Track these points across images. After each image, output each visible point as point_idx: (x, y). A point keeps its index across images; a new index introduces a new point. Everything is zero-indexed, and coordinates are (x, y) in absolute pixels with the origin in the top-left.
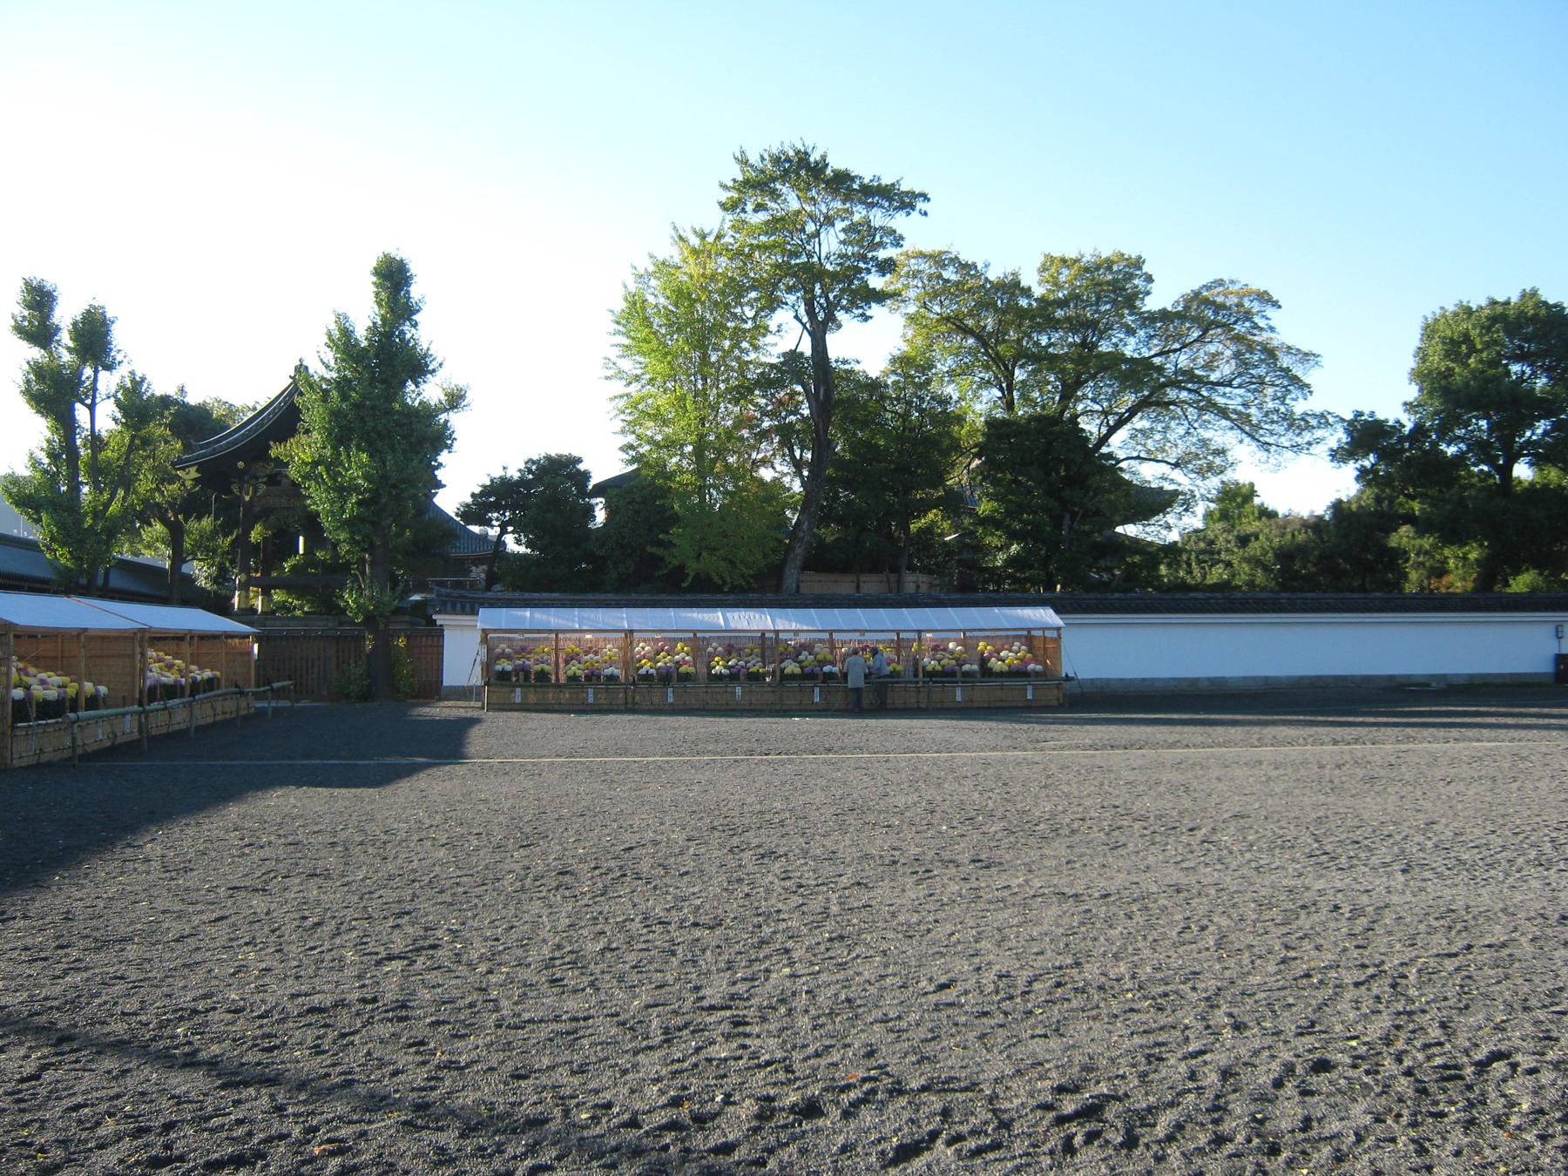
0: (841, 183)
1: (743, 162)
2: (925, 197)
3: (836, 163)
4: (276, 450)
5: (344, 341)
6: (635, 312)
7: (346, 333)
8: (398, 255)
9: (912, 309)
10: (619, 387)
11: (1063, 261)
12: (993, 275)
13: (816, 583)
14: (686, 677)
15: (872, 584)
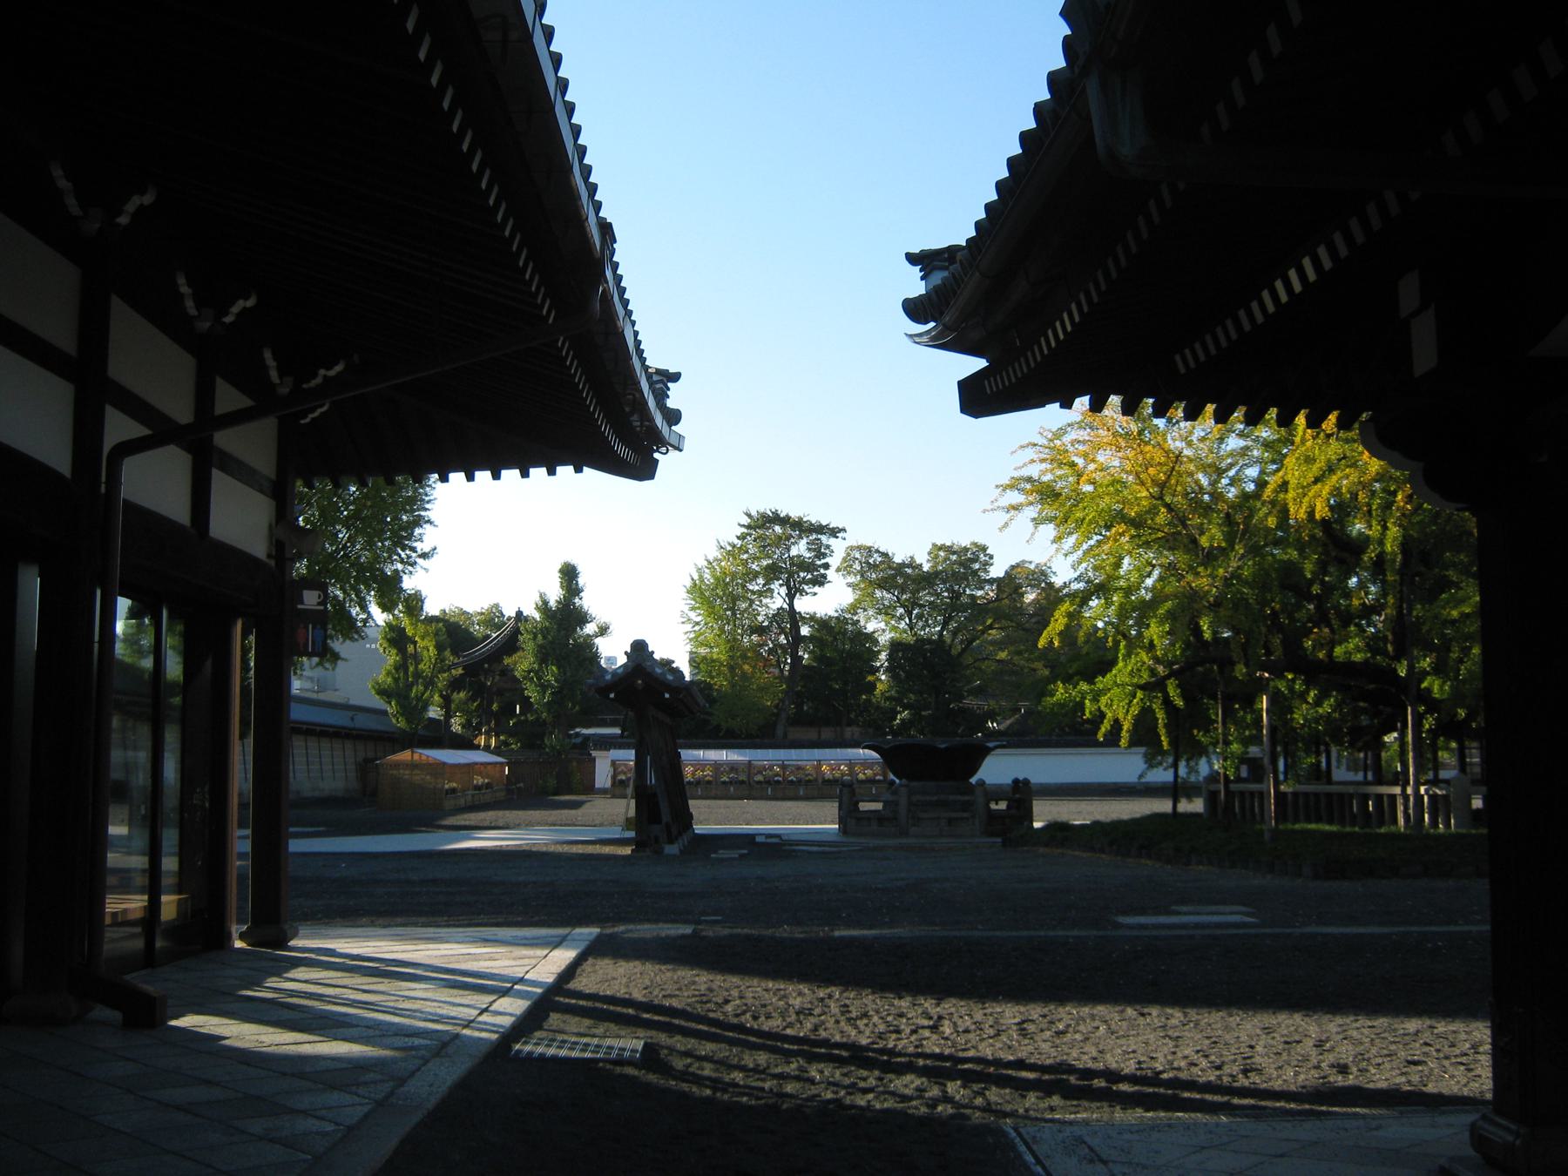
0: (801, 527)
1: (749, 516)
2: (844, 530)
3: (794, 514)
4: (507, 661)
5: (544, 607)
6: (696, 590)
7: (545, 603)
8: (573, 562)
9: (851, 579)
10: (688, 627)
11: (940, 548)
12: (898, 559)
13: (797, 733)
14: (709, 782)
15: (827, 733)
